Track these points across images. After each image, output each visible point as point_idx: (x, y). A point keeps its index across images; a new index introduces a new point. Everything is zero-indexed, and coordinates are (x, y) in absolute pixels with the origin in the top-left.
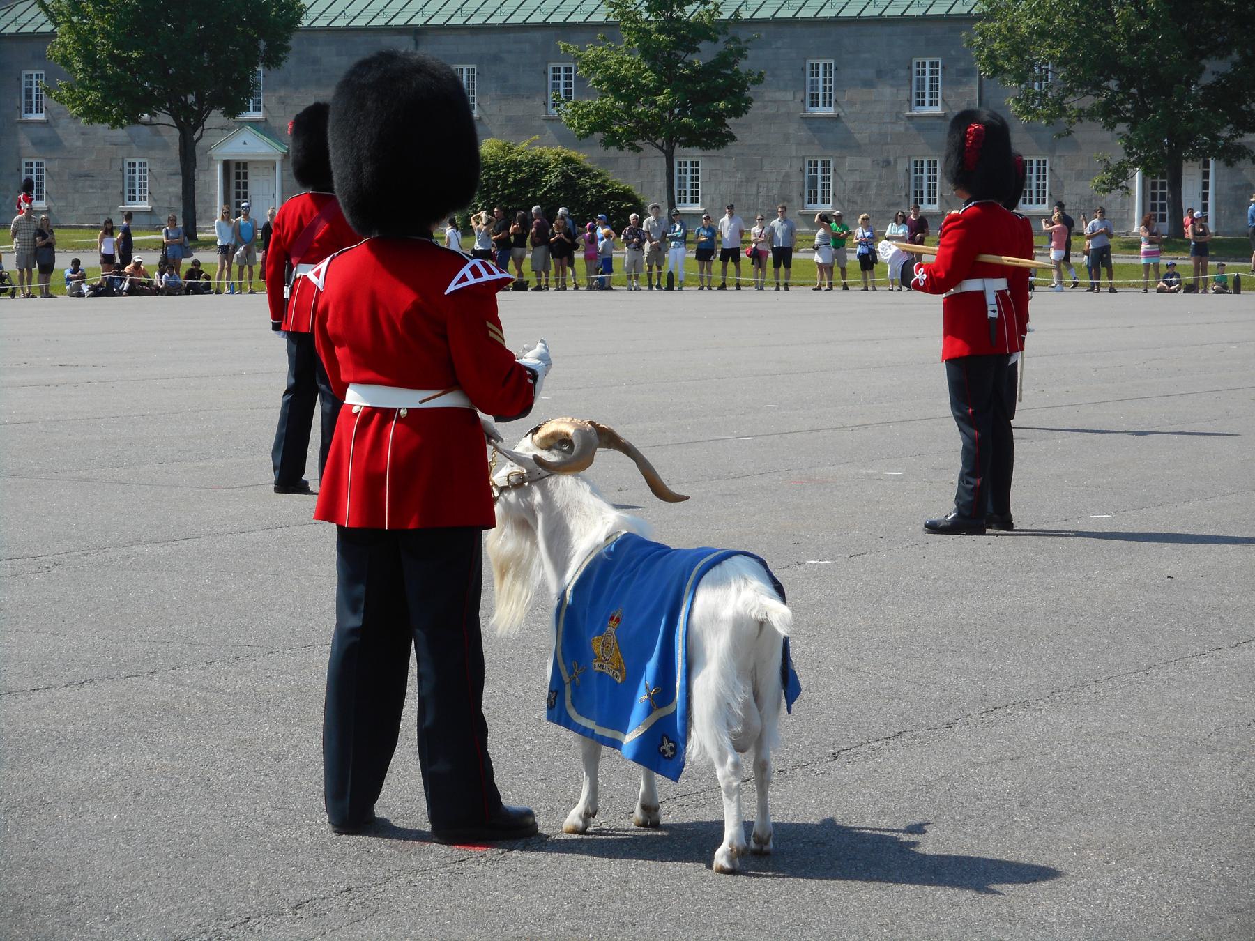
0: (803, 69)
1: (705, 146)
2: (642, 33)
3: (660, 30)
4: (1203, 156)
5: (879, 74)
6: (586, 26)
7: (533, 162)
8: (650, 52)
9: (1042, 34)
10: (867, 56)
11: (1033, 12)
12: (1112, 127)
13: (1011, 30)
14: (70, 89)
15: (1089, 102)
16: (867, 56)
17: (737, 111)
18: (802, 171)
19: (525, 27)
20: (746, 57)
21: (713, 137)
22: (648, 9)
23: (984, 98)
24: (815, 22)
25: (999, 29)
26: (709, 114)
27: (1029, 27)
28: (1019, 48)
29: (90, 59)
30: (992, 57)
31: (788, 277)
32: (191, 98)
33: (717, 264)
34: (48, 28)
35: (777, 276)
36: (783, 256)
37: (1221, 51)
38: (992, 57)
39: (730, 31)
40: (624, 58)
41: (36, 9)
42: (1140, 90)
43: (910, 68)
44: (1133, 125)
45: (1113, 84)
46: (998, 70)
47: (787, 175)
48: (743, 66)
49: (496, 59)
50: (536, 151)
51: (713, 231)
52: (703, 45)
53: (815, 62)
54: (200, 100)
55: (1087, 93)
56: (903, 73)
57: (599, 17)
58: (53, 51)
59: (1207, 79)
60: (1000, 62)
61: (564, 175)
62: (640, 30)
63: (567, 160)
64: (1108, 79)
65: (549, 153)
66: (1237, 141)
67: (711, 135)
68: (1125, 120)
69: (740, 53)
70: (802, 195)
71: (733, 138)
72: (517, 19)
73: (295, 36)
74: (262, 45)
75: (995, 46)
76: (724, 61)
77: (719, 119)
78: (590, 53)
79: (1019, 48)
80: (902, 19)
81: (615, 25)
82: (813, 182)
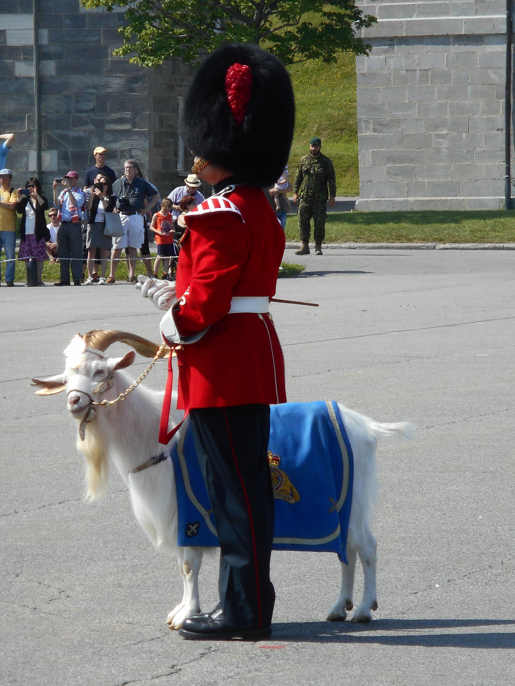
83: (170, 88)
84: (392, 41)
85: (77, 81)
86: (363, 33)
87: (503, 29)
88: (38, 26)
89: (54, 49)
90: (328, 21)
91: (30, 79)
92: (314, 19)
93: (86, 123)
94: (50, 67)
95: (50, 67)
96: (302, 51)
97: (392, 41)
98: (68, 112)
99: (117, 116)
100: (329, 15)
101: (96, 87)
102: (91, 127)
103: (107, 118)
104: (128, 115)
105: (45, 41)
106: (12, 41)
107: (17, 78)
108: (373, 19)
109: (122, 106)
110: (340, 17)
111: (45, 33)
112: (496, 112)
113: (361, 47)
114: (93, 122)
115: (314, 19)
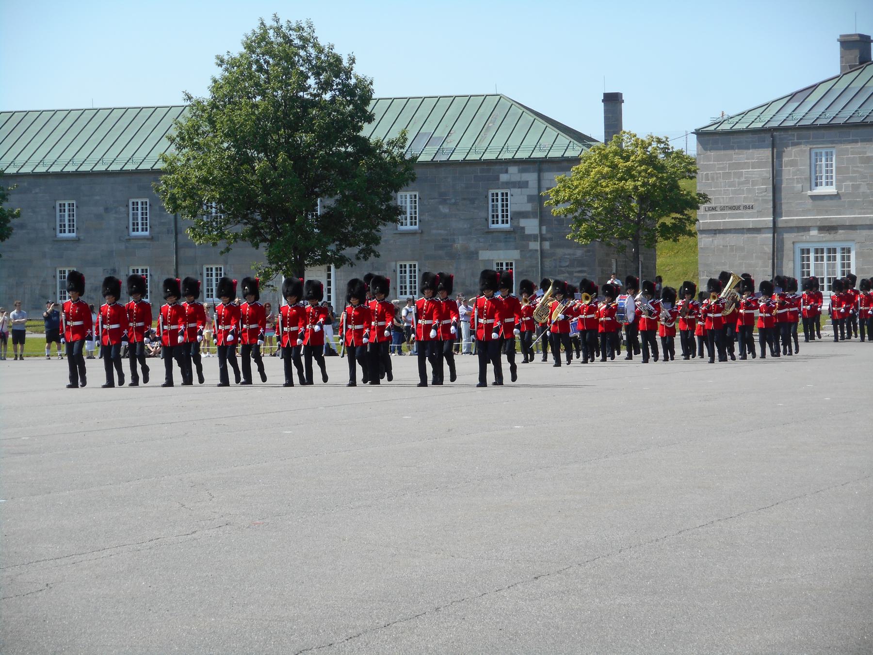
0: (54, 208)
5: (107, 210)
9: (205, 181)
10: (98, 198)
11: (200, 168)
12: (257, 246)
15: (240, 228)
16: (98, 198)
18: (55, 277)
20: (7, 200)
23: (179, 225)
25: (178, 179)
27: (196, 177)
28: (191, 194)
30: (173, 199)
31: (22, 350)
35: (16, 350)
36: (19, 337)
37: (328, 192)
38: (173, 199)
42: (274, 219)
43: (127, 206)
46: (176, 208)
47: (44, 281)
53: (62, 202)
55: (239, 222)
56: (123, 209)
59: (319, 211)
60: (179, 202)
66: (342, 252)
70: (55, 293)
75: (175, 191)
79: (191, 194)
80: (122, 173)
83: (608, 255)
84: (715, 232)
85: (560, 252)
86: (693, 228)
87: (771, 225)
88: (541, 225)
89: (549, 236)
90: (673, 221)
91: (537, 250)
92: (668, 221)
93: (563, 272)
94: (547, 245)
95: (547, 245)
96: (662, 236)
97: (715, 232)
98: (555, 267)
99: (580, 269)
100: (675, 218)
101: (569, 254)
102: (567, 275)
103: (574, 270)
104: (585, 269)
105: (544, 232)
106: (527, 232)
107: (531, 250)
108: (697, 220)
109: (583, 265)
110: (680, 219)
111: (544, 228)
112: (767, 267)
113: (691, 234)
114: (569, 272)
115: (668, 221)
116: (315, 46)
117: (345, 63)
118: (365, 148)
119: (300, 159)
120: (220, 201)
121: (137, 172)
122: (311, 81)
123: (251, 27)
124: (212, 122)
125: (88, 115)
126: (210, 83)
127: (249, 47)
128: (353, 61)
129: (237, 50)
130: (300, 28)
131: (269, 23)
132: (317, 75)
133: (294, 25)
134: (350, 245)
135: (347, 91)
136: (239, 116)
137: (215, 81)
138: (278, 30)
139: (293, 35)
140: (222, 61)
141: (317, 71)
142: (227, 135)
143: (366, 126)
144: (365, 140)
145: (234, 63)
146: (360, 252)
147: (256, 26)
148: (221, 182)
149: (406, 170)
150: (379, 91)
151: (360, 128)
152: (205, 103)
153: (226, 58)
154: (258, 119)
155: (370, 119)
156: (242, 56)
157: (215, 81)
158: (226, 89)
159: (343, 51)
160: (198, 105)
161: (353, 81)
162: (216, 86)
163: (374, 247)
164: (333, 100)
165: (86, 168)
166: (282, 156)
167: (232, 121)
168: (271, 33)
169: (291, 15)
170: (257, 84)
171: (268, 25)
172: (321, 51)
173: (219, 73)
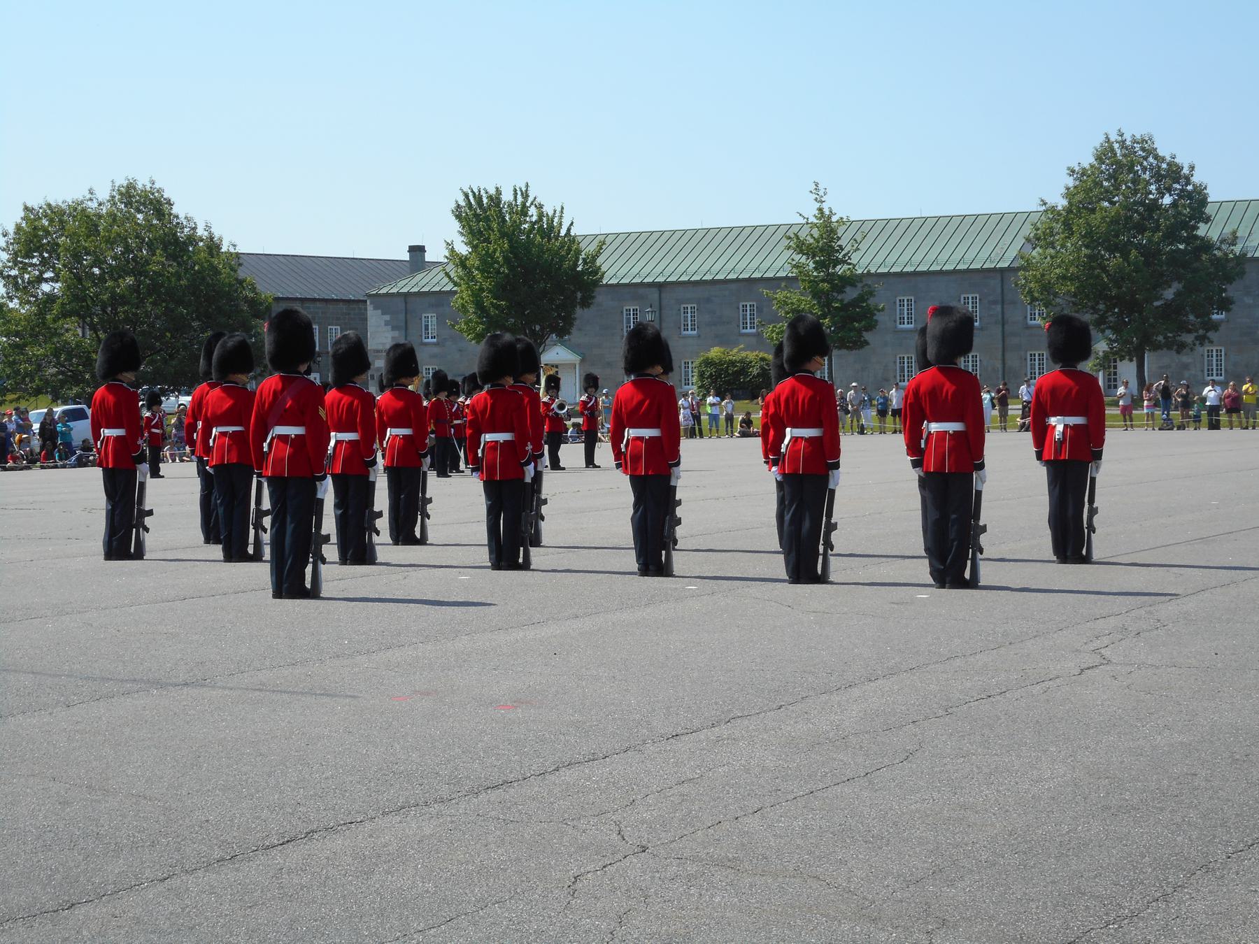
1: (848, 348)
2: (814, 283)
3: (823, 281)
4: (1156, 347)
6: (774, 282)
7: (742, 361)
8: (816, 294)
9: (1064, 277)
12: (1103, 331)
13: (1043, 275)
14: (466, 323)
17: (870, 327)
19: (725, 281)
21: (859, 344)
22: (816, 269)
24: (901, 275)
26: (854, 329)
28: (1046, 288)
29: (479, 306)
32: (538, 328)
33: (889, 418)
34: (449, 287)
38: (1030, 292)
39: (865, 281)
40: (803, 300)
41: (442, 274)
44: (1116, 329)
45: (1101, 307)
46: (1034, 299)
48: (872, 301)
49: (708, 300)
50: (744, 354)
51: (887, 400)
52: (848, 289)
54: (542, 329)
57: (782, 274)
58: (456, 302)
60: (1036, 295)
61: (762, 368)
62: (810, 282)
63: (763, 359)
64: (1098, 303)
65: (751, 356)
67: (855, 343)
68: (1109, 328)
69: (871, 294)
71: (867, 343)
72: (720, 277)
73: (597, 289)
74: (579, 295)
75: (1032, 285)
76: (862, 298)
77: (859, 331)
78: (780, 295)
79: (1046, 288)
80: (955, 271)
81: (795, 279)
82: (902, 370)
116: (1156, 157)
117: (1186, 171)
118: (1206, 246)
119: (1150, 254)
120: (1075, 295)
121: (968, 271)
122: (1153, 187)
123: (1098, 141)
124: (1067, 225)
125: (917, 223)
126: (1064, 191)
127: (1100, 158)
128: (1192, 168)
129: (1088, 160)
130: (1143, 141)
131: (1113, 137)
132: (1158, 181)
133: (1138, 137)
134: (1189, 331)
135: (1183, 194)
136: (1095, 219)
137: (1068, 189)
138: (1122, 143)
139: (1137, 147)
140: (1073, 171)
141: (1158, 176)
142: (1083, 237)
143: (1201, 225)
144: (1202, 239)
145: (1084, 172)
146: (1197, 338)
147: (1102, 138)
148: (1078, 277)
149: (1238, 265)
150: (1214, 195)
151: (1196, 228)
152: (1060, 208)
153: (1077, 169)
154: (1111, 222)
155: (1207, 220)
156: (1092, 166)
157: (1068, 189)
158: (1081, 196)
159: (1183, 160)
160: (1053, 209)
161: (1190, 188)
162: (1069, 194)
163: (1211, 334)
164: (1174, 204)
165: (923, 268)
166: (1134, 253)
167: (1088, 224)
168: (1116, 146)
169: (1133, 130)
170: (1107, 191)
171: (1112, 139)
172: (1163, 159)
173: (1071, 182)
